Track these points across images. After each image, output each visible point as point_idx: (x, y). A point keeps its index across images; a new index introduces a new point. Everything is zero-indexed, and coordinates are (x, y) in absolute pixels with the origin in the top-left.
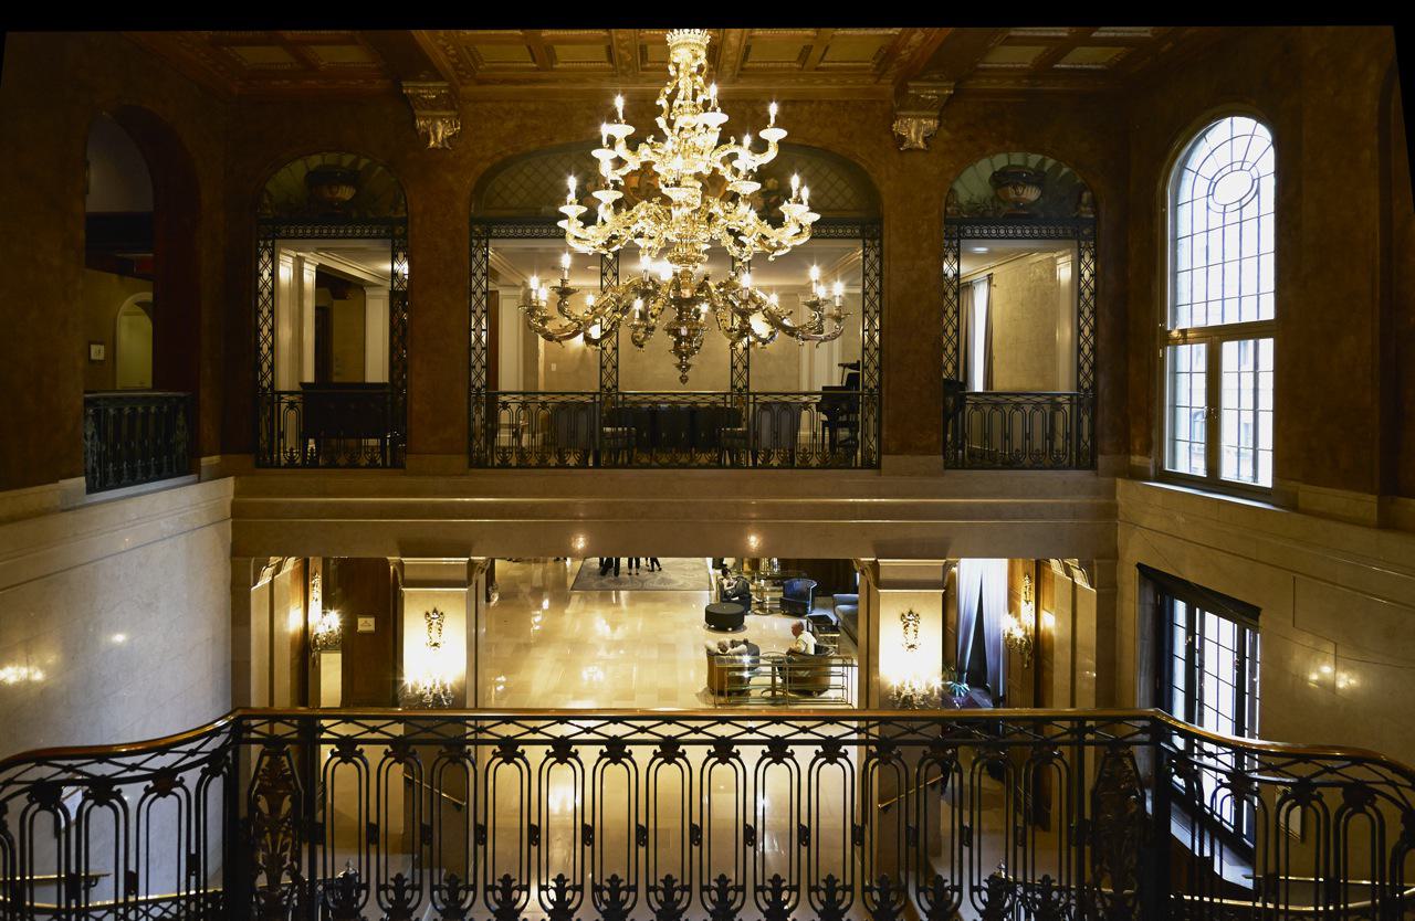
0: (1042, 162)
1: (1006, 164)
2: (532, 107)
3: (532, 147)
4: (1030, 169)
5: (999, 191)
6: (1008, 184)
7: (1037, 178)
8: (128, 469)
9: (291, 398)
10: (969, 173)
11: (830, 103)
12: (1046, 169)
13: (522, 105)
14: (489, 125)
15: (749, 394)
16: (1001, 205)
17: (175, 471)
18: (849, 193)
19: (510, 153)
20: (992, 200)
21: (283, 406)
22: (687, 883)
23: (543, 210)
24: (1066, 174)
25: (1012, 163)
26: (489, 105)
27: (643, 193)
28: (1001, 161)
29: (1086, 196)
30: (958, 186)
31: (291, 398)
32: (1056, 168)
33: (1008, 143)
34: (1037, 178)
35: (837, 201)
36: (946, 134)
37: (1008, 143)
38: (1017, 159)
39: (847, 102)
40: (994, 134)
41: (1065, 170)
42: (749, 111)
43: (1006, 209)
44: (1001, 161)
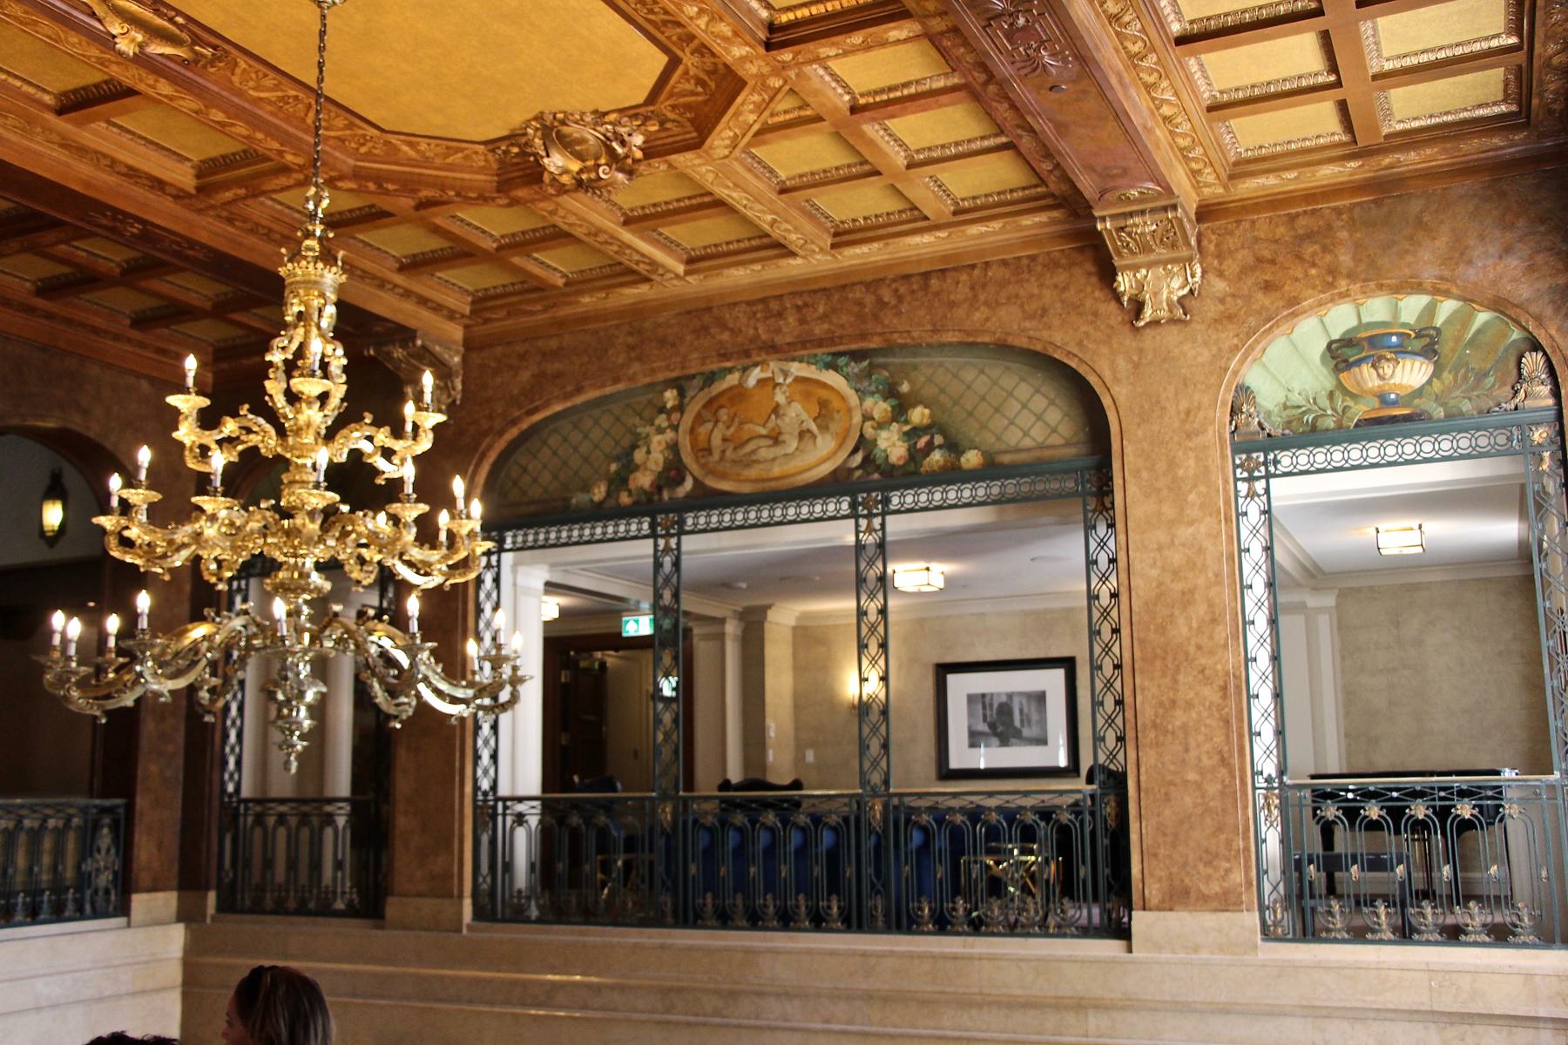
0: (1430, 310)
1: (1352, 322)
2: (554, 343)
4: (1405, 325)
5: (1343, 376)
6: (1358, 363)
7: (1426, 342)
8: (50, 901)
10: (1277, 349)
11: (1004, 263)
12: (1439, 322)
13: (541, 343)
14: (498, 380)
15: (497, 799)
16: (1350, 403)
17: (88, 907)
18: (1054, 416)
20: (1331, 395)
21: (509, 820)
23: (574, 501)
24: (1486, 324)
25: (1365, 320)
26: (498, 350)
28: (1341, 318)
29: (1533, 362)
30: (1254, 377)
32: (1463, 319)
33: (1343, 284)
34: (1426, 342)
35: (1033, 433)
36: (1220, 286)
37: (1343, 284)
38: (1377, 309)
39: (1033, 258)
40: (1313, 272)
41: (1483, 317)
42: (869, 299)
43: (1360, 410)
44: (1341, 318)
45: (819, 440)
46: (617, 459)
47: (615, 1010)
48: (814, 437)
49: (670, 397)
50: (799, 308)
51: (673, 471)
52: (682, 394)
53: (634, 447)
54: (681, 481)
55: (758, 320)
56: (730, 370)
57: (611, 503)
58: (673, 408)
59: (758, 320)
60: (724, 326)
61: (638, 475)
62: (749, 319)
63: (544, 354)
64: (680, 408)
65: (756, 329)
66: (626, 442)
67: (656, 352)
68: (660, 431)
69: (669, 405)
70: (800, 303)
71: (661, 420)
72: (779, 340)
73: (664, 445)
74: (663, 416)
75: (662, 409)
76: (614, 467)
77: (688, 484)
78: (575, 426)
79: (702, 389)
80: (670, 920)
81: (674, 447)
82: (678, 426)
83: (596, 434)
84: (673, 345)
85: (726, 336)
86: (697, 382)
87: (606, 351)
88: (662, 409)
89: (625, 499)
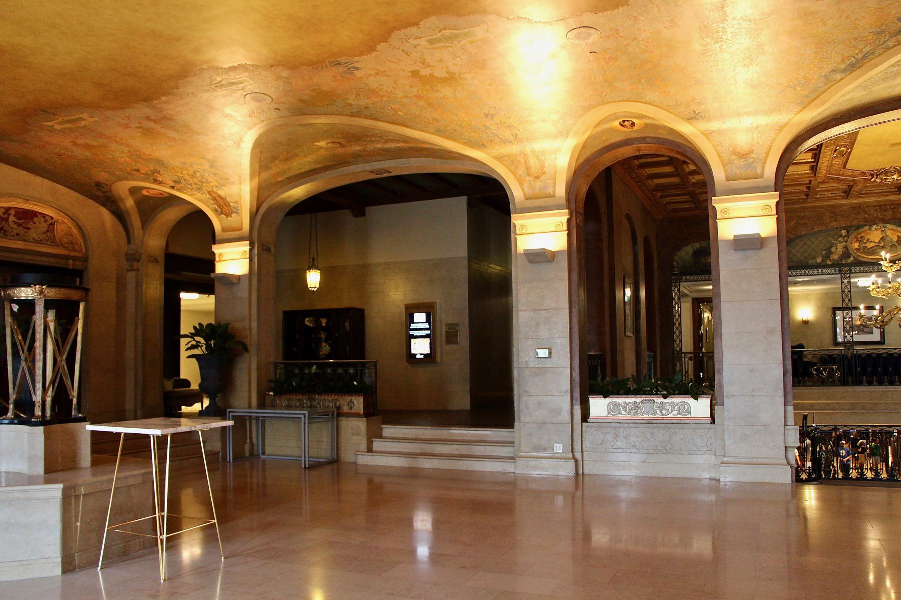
2: (802, 214)
3: (803, 233)
9: (690, 355)
13: (797, 214)
19: (792, 237)
22: (882, 468)
23: (810, 262)
27: (862, 251)
31: (690, 355)
45: (898, 248)
46: (826, 250)
47: (836, 410)
48: (897, 247)
49: (844, 232)
50: (893, 209)
51: (847, 254)
52: (848, 232)
53: (831, 247)
54: (850, 258)
55: (878, 212)
56: (866, 226)
57: (823, 264)
58: (845, 236)
59: (878, 212)
60: (866, 213)
61: (834, 255)
62: (875, 211)
63: (799, 217)
64: (848, 236)
65: (878, 214)
66: (828, 245)
67: (841, 219)
68: (841, 243)
69: (844, 235)
70: (893, 207)
71: (841, 239)
72: (886, 218)
73: (842, 247)
74: (841, 238)
75: (841, 236)
76: (824, 253)
77: (852, 259)
78: (809, 239)
79: (856, 231)
80: (851, 384)
81: (846, 248)
82: (847, 241)
83: (817, 242)
84: (848, 217)
85: (866, 216)
86: (854, 229)
87: (823, 218)
88: (841, 236)
89: (829, 263)
